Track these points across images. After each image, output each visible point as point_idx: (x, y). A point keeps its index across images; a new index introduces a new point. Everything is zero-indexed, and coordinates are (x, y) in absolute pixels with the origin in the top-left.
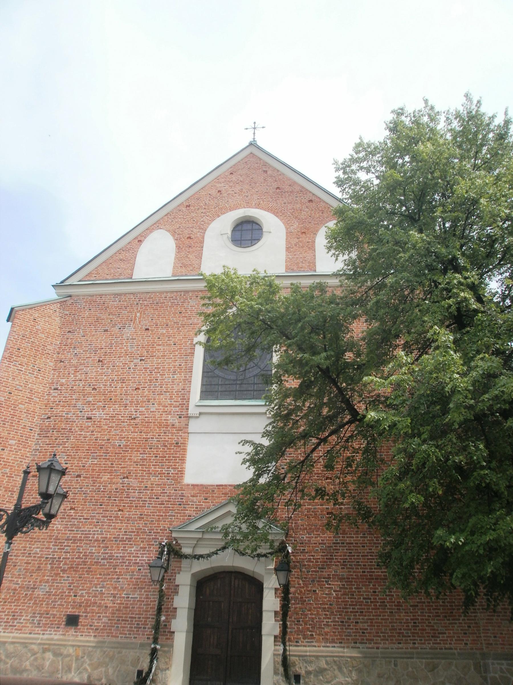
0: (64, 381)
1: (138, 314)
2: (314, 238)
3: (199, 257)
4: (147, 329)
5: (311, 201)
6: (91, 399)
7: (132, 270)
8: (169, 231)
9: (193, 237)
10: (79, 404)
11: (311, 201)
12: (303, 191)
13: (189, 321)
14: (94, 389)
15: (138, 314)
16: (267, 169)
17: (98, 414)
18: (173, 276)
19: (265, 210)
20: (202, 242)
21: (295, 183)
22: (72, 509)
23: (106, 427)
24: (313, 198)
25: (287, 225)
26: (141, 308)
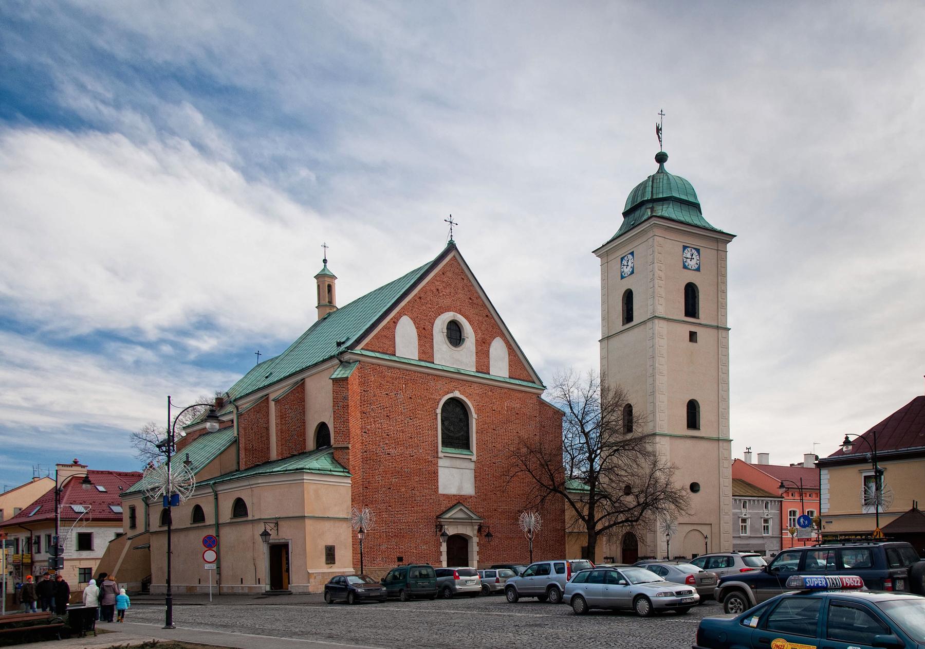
0: (369, 427)
1: (404, 386)
2: (489, 348)
3: (432, 347)
4: (411, 398)
5: (487, 316)
6: (387, 442)
7: (394, 347)
8: (411, 319)
9: (426, 329)
10: (381, 444)
11: (487, 316)
12: (484, 305)
13: (432, 396)
14: (388, 435)
15: (404, 386)
16: (463, 277)
17: (392, 451)
18: (420, 360)
19: (464, 316)
20: (432, 335)
21: (479, 297)
22: (389, 506)
23: (398, 460)
24: (489, 314)
25: (475, 332)
26: (405, 381)
